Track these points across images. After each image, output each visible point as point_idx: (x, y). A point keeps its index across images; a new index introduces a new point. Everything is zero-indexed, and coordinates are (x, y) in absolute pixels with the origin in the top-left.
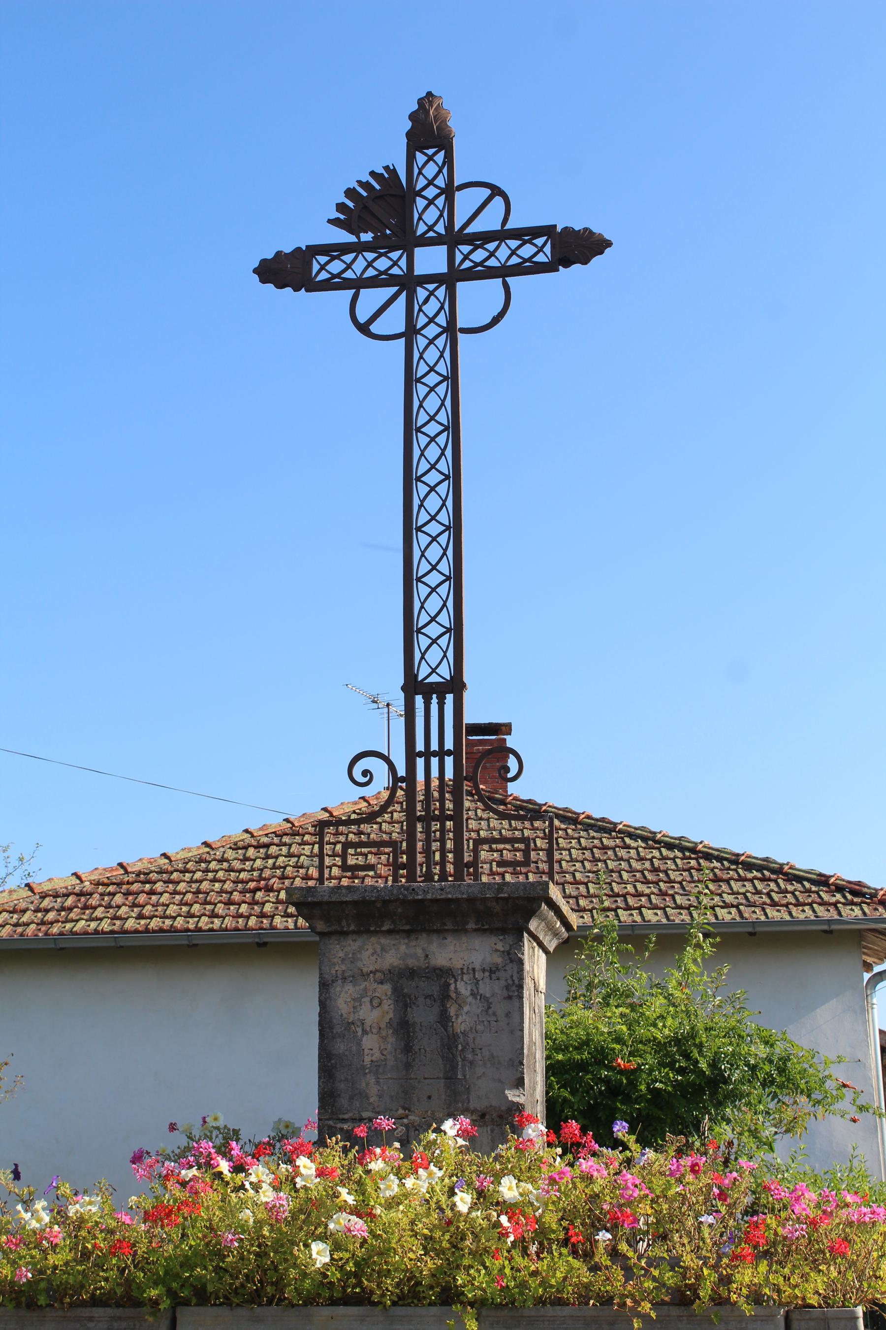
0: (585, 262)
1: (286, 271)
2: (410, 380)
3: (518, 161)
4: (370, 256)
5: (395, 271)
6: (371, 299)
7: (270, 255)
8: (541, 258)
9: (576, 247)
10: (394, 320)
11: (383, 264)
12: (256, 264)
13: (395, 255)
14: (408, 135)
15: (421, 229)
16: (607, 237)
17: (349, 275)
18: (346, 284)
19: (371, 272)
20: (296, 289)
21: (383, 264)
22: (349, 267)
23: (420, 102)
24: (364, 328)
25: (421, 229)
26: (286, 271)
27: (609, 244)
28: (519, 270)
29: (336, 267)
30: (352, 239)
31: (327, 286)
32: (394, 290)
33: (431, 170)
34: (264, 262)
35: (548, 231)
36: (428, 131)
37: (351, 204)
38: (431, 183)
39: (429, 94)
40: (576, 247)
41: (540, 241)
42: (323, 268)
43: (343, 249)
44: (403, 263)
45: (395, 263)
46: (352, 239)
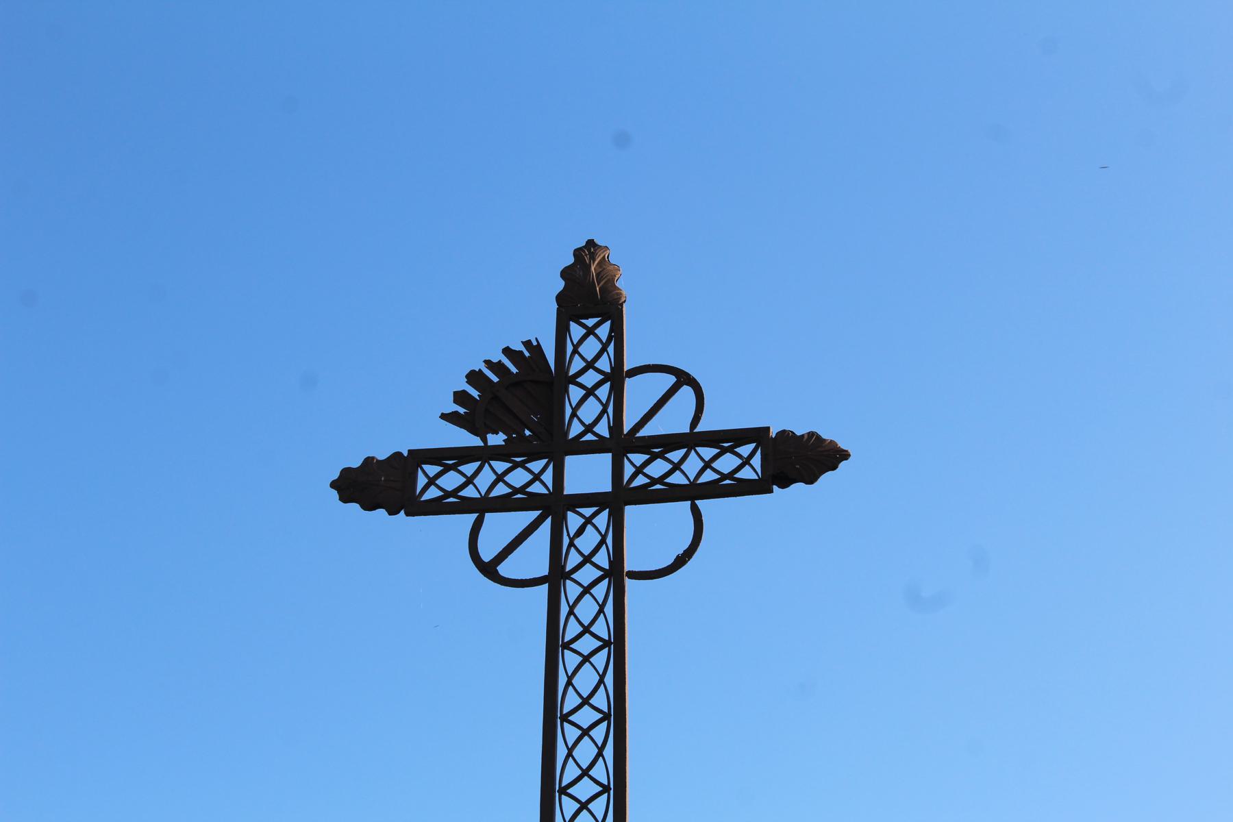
0: (810, 480)
1: (380, 485)
2: (555, 645)
3: (713, 337)
4: (501, 466)
5: (537, 488)
6: (500, 528)
7: (356, 463)
8: (746, 474)
9: (798, 459)
10: (533, 559)
11: (519, 478)
12: (336, 476)
13: (536, 466)
14: (560, 298)
15: (576, 429)
16: (843, 445)
17: (470, 492)
18: (466, 506)
19: (501, 490)
20: (393, 512)
21: (519, 478)
22: (469, 481)
23: (578, 253)
24: (489, 570)
25: (576, 429)
26: (380, 485)
27: (845, 455)
28: (715, 490)
29: (451, 481)
30: (476, 441)
31: (437, 507)
32: (535, 514)
33: (590, 348)
34: (346, 472)
35: (757, 435)
36: (588, 292)
37: (475, 393)
38: (590, 365)
39: (591, 243)
40: (798, 459)
41: (745, 450)
42: (432, 482)
43: (462, 455)
44: (548, 477)
45: (537, 477)
46: (476, 441)
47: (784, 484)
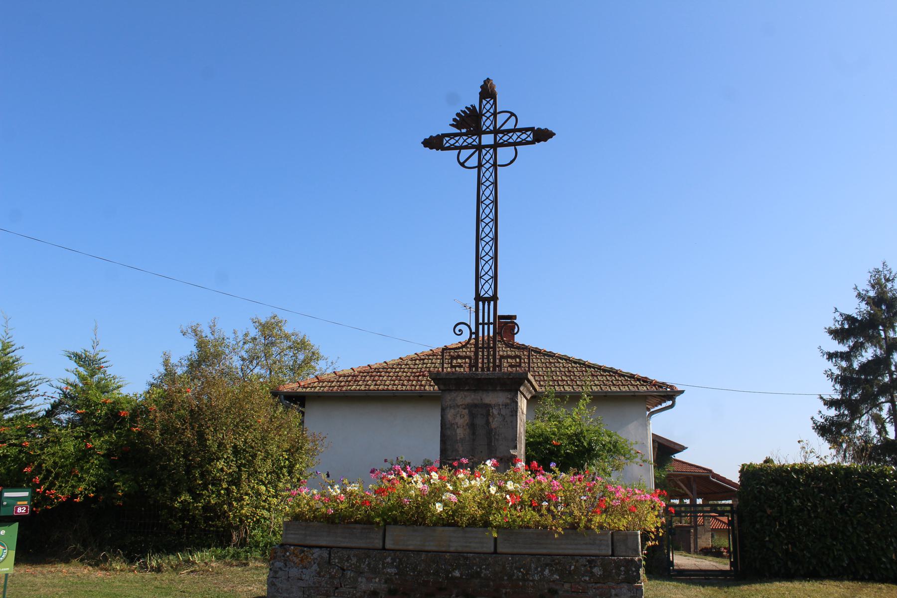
0: (545, 141)
1: (434, 143)
2: (479, 184)
3: (520, 104)
4: (465, 138)
5: (474, 143)
6: (465, 153)
9: (542, 135)
10: (474, 161)
11: (470, 141)
13: (474, 137)
14: (480, 93)
15: (484, 128)
17: (457, 144)
18: (456, 148)
19: (465, 144)
21: (470, 141)
23: (485, 81)
24: (462, 164)
25: (484, 128)
26: (434, 143)
27: (554, 134)
29: (452, 141)
30: (459, 131)
31: (449, 148)
33: (488, 106)
35: (532, 129)
36: (487, 92)
38: (488, 111)
40: (542, 135)
41: (528, 133)
43: (455, 135)
44: (477, 140)
46: (459, 131)
47: (539, 142)
